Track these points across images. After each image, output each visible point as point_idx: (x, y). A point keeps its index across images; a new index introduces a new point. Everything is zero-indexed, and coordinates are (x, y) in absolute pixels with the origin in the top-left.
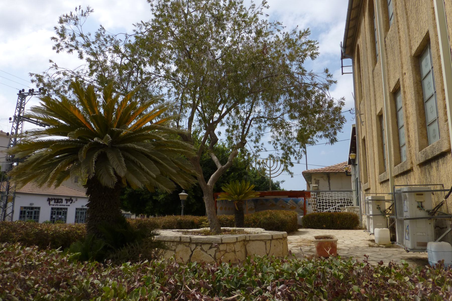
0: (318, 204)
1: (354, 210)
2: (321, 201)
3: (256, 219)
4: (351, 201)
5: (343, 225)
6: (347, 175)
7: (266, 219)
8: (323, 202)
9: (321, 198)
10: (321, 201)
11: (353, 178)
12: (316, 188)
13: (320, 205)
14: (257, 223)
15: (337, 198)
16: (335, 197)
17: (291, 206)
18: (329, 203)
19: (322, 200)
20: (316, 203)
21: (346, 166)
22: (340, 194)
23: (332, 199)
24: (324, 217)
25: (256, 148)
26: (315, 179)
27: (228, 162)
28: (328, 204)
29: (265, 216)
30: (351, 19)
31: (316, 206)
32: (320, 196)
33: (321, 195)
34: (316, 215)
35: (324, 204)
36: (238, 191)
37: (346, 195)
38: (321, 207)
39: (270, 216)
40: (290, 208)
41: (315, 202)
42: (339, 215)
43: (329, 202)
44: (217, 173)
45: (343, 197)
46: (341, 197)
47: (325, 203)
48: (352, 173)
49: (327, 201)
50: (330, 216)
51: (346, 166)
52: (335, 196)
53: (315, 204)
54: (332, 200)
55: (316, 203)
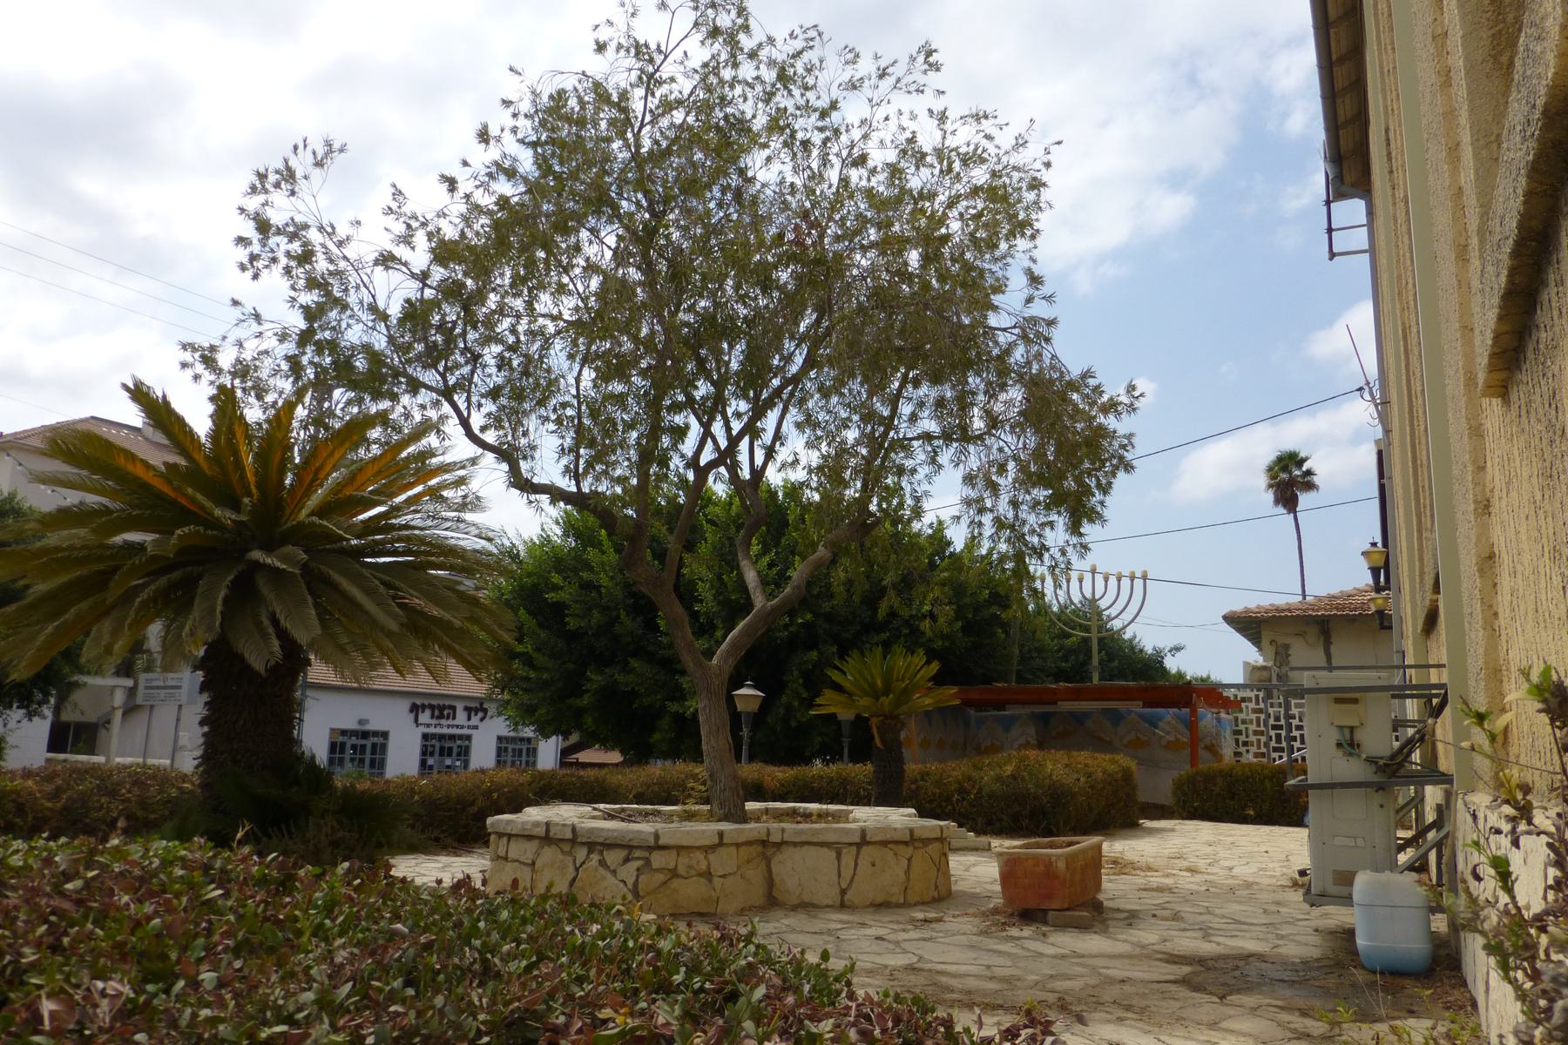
3: (969, 779)
6: (1383, 627)
7: (999, 779)
12: (1265, 674)
14: (968, 793)
20: (1262, 728)
24: (1248, 778)
26: (1271, 642)
30: (1334, 57)
31: (1263, 739)
36: (879, 682)
40: (1165, 747)
44: (748, 626)
50: (1271, 778)
53: (1262, 733)
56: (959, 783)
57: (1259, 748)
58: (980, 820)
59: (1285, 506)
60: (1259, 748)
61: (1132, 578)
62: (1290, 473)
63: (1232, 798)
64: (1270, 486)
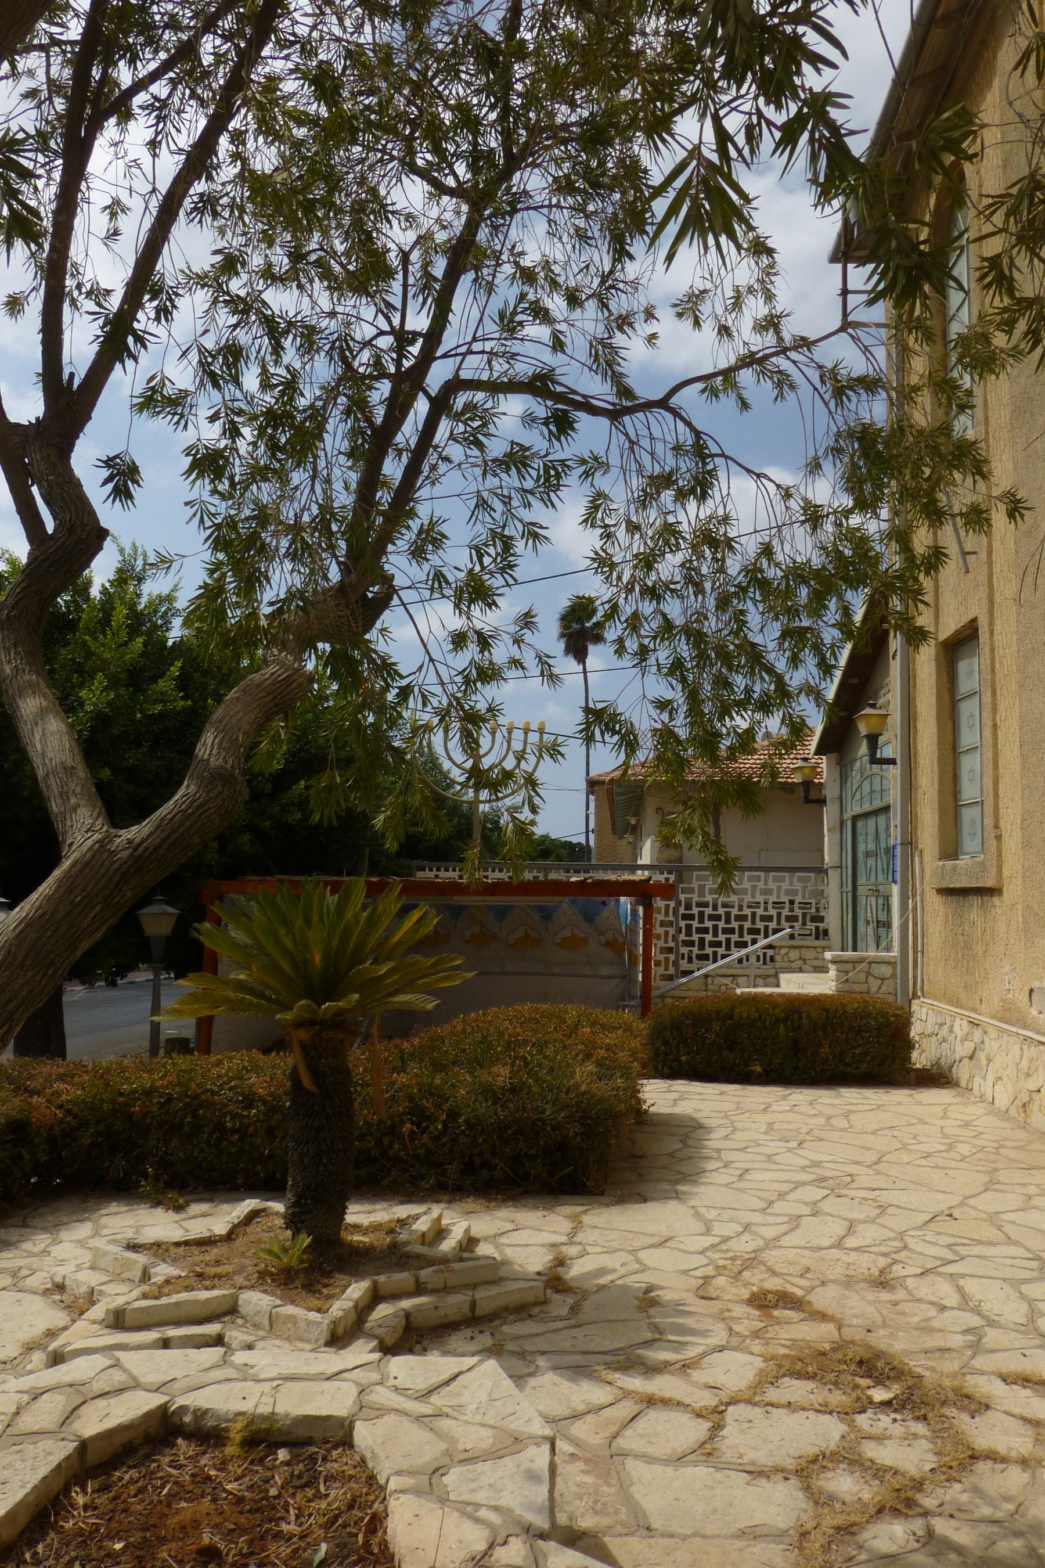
0: (682, 924)
1: (868, 974)
2: (695, 911)
3: (430, 1092)
4: (818, 910)
5: (847, 1065)
6: (808, 800)
7: (488, 1092)
8: (701, 914)
9: (695, 898)
10: (695, 911)
11: (829, 816)
13: (689, 927)
14: (432, 1119)
15: (760, 898)
16: (753, 896)
17: (568, 933)
18: (728, 921)
19: (698, 905)
20: (671, 918)
21: (805, 760)
22: (775, 880)
23: (741, 900)
25: (472, 651)
26: (658, 810)
27: (186, 790)
28: (722, 924)
29: (484, 1077)
30: (939, 13)
31: (672, 931)
32: (691, 891)
33: (695, 885)
34: (718, 1012)
35: (709, 924)
36: (318, 958)
37: (798, 886)
38: (695, 937)
39: (514, 1074)
41: (667, 914)
42: (826, 1010)
43: (728, 915)
45: (788, 892)
46: (778, 897)
47: (711, 918)
48: (831, 792)
49: (721, 911)
50: (785, 1020)
51: (805, 760)
52: (754, 888)
53: (671, 923)
54: (741, 908)
55: (671, 918)
56: (410, 1098)
57: (666, 942)
58: (453, 1169)
59: (575, 657)
60: (666, 942)
61: (527, 731)
62: (583, 624)
63: (731, 1048)
64: (562, 635)
